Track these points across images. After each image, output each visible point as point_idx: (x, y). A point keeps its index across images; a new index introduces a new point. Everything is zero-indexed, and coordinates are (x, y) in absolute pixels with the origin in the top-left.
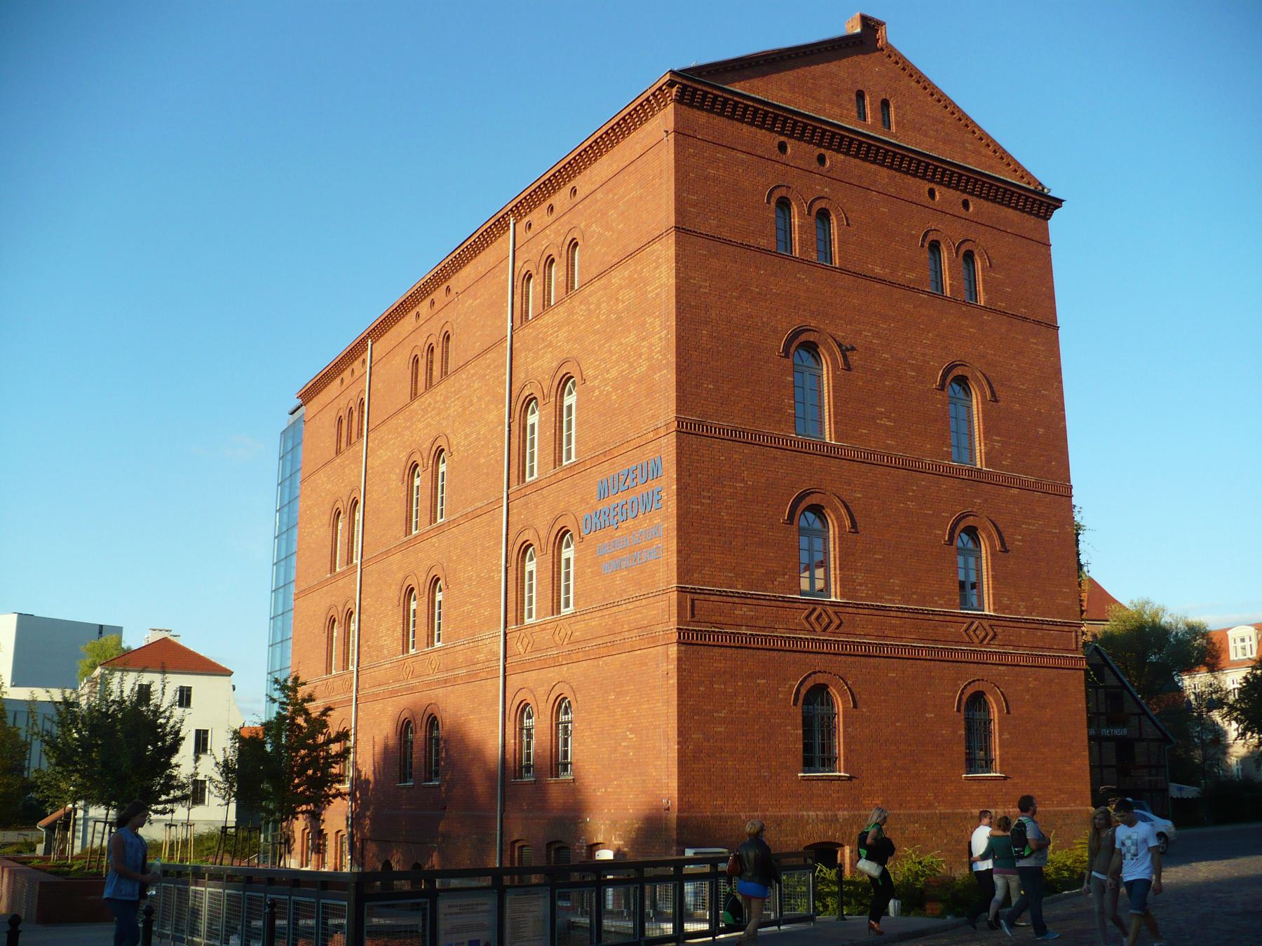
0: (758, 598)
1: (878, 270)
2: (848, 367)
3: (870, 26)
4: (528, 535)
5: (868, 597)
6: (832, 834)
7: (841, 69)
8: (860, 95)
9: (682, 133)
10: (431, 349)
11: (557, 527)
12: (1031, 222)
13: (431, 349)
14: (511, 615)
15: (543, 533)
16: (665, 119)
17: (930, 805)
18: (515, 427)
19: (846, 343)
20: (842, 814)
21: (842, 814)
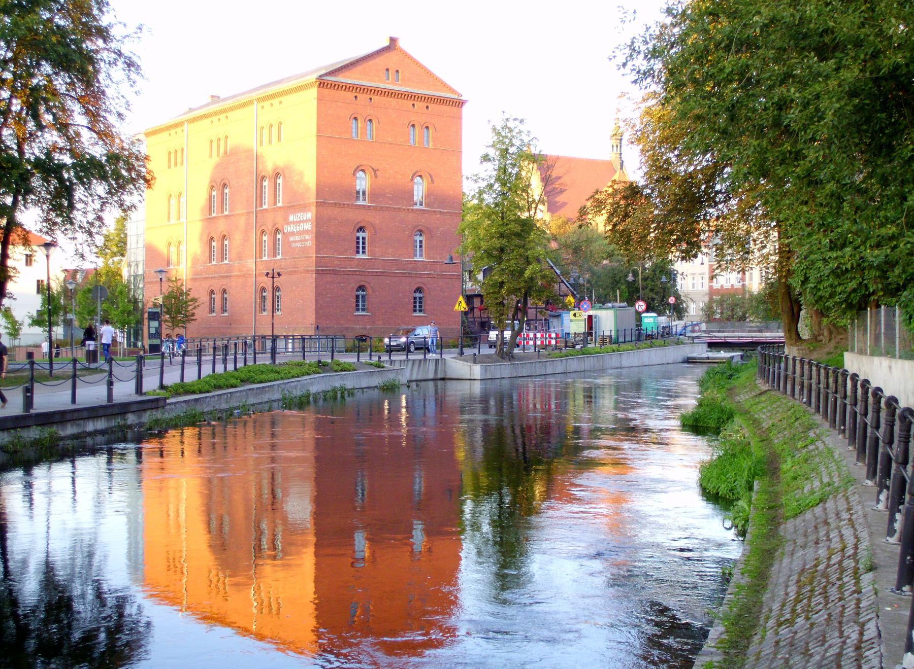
0: (341, 258)
1: (390, 139)
2: (376, 177)
3: (393, 40)
4: (264, 228)
5: (380, 256)
6: (364, 333)
7: (380, 61)
8: (387, 70)
9: (320, 99)
10: (219, 139)
11: (275, 227)
12: (455, 109)
13: (219, 139)
14: (258, 255)
15: (270, 228)
16: (314, 92)
17: (399, 325)
18: (258, 186)
19: (375, 168)
20: (368, 327)
21: (368, 327)
